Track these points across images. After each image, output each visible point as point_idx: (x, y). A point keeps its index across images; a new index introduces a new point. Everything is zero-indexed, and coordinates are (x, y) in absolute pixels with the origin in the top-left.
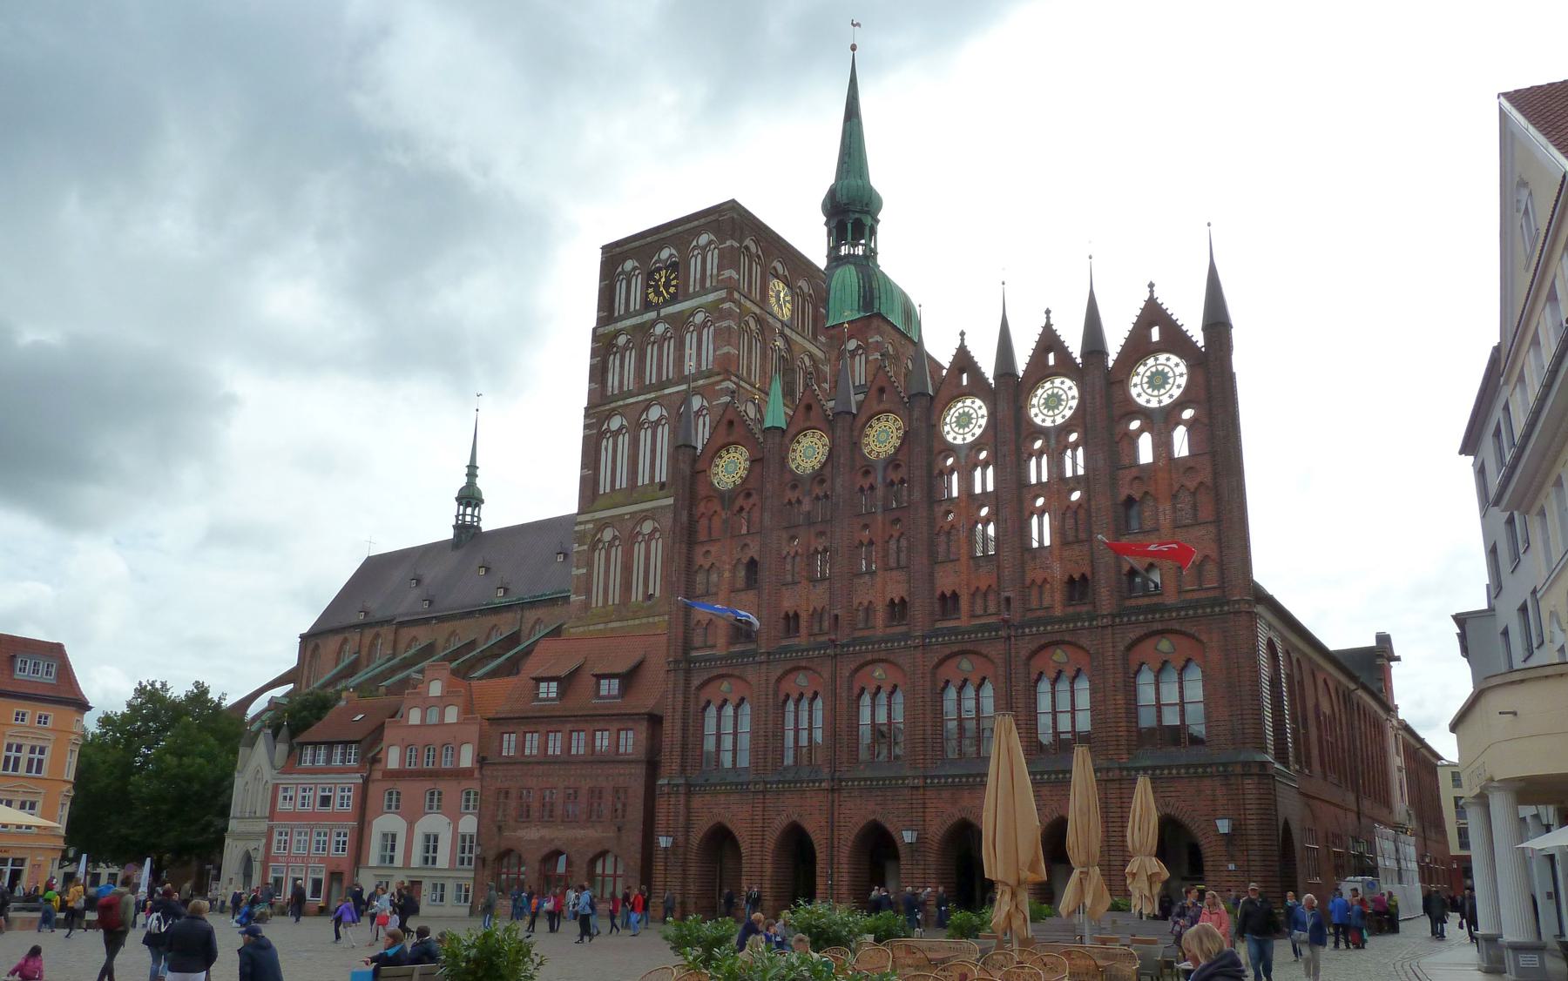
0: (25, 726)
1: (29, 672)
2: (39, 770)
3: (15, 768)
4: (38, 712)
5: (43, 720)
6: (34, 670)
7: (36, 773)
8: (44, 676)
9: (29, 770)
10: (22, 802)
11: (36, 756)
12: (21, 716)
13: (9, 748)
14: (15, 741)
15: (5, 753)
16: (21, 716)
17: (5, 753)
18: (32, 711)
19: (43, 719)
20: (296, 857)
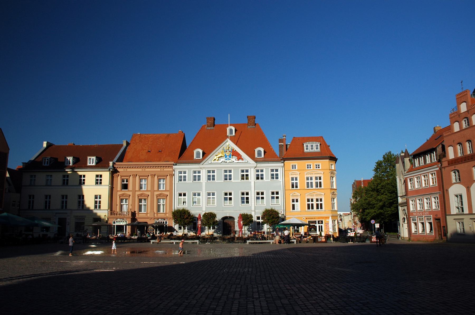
0: (311, 170)
1: (310, 150)
2: (320, 186)
3: (312, 186)
4: (315, 164)
5: (309, 167)
6: (311, 148)
7: (320, 187)
8: (311, 150)
9: (317, 186)
10: (316, 199)
11: (318, 181)
12: (309, 166)
13: (308, 179)
14: (309, 176)
15: (306, 181)
16: (309, 166)
17: (306, 181)
18: (313, 163)
19: (318, 166)
20: (420, 212)
